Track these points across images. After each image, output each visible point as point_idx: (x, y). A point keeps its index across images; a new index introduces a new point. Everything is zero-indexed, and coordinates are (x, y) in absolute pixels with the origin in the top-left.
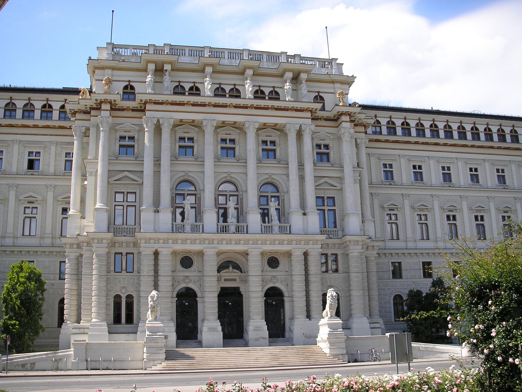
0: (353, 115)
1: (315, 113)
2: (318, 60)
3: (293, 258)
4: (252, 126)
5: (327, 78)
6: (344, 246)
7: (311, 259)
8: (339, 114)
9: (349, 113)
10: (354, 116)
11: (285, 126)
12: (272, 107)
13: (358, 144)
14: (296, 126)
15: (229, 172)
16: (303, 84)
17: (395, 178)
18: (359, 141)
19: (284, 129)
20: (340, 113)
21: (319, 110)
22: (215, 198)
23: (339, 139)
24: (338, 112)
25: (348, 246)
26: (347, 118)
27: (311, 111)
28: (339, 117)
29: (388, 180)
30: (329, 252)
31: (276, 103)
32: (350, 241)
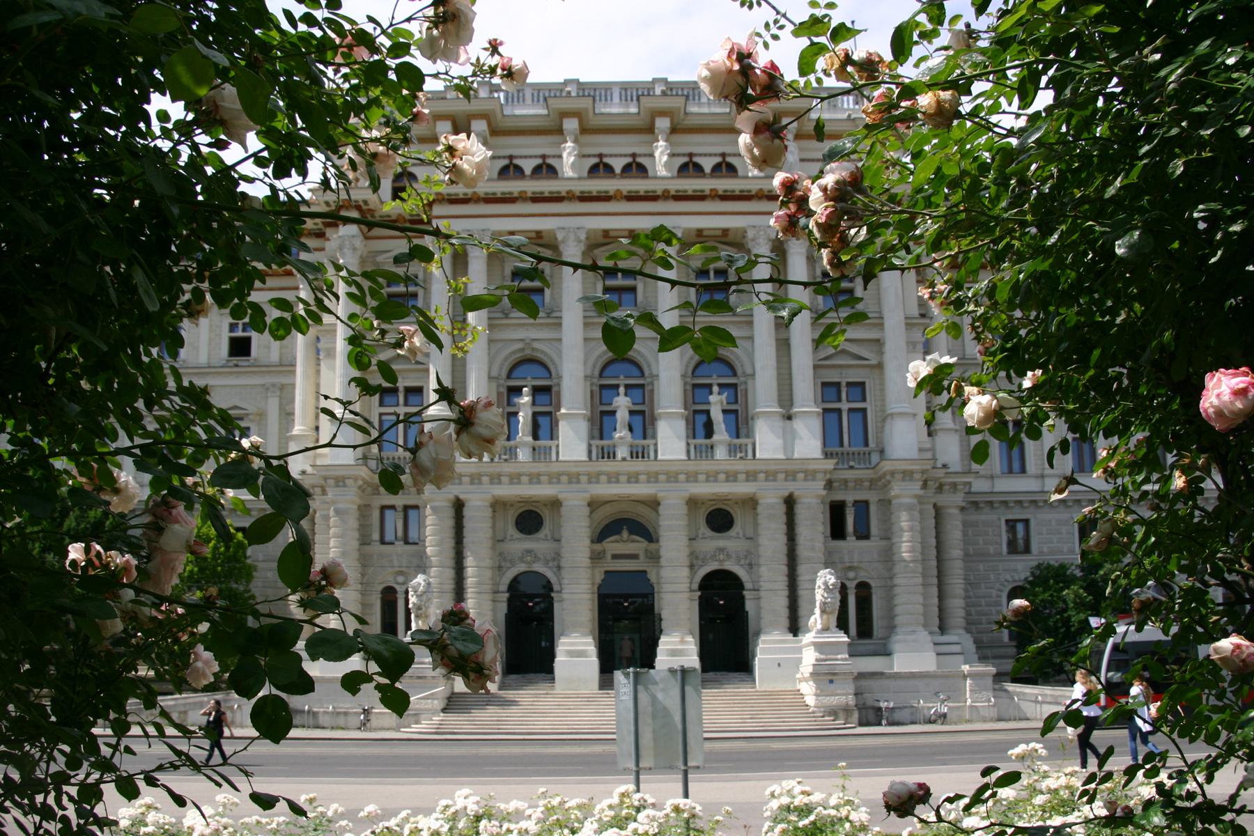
3: (760, 509)
6: (880, 483)
7: (801, 512)
12: (713, 193)
25: (889, 482)
30: (849, 498)
31: (723, 184)
32: (893, 473)
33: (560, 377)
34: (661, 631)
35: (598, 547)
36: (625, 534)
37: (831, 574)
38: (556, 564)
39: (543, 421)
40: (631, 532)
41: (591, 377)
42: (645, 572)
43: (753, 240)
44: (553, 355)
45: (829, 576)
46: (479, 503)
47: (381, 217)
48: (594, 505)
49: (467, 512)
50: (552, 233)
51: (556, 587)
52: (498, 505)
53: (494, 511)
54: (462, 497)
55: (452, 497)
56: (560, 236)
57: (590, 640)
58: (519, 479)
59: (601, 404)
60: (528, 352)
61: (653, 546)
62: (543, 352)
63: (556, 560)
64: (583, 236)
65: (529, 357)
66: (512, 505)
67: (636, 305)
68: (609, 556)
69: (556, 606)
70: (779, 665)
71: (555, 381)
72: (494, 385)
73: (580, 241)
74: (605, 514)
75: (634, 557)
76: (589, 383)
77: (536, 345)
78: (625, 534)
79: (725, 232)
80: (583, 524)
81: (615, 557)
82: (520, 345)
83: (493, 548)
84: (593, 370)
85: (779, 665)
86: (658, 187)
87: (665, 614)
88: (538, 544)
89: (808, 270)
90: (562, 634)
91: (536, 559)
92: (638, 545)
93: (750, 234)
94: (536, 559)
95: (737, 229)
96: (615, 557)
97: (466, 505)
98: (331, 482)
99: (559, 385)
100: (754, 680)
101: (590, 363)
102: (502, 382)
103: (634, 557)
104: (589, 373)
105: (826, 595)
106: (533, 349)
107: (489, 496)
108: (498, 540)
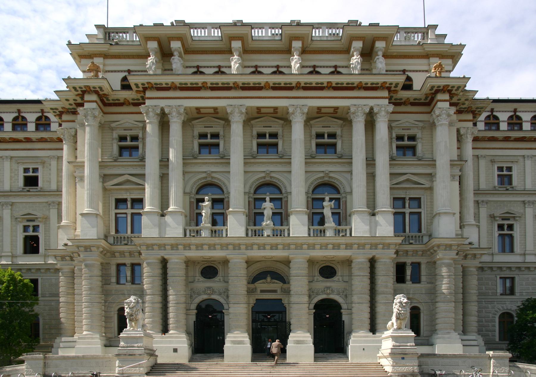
0: (456, 92)
1: (396, 92)
2: (406, 31)
4: (299, 110)
5: (418, 50)
8: (433, 91)
9: (449, 88)
10: (457, 95)
11: (349, 111)
13: (462, 136)
14: (364, 108)
15: (267, 170)
16: (378, 56)
17: (515, 182)
18: (462, 132)
19: (348, 116)
20: (435, 89)
21: (400, 86)
22: (249, 202)
23: (432, 126)
24: (432, 87)
26: (447, 96)
27: (389, 89)
28: (433, 96)
29: (504, 185)
33: (229, 193)
34: (290, 331)
35: (252, 286)
36: (269, 279)
37: (404, 297)
38: (226, 294)
39: (219, 219)
40: (272, 278)
41: (249, 193)
42: (281, 300)
43: (353, 113)
44: (226, 182)
45: (403, 298)
46: (176, 261)
47: (113, 100)
48: (249, 263)
49: (169, 265)
50: (224, 108)
51: (226, 306)
52: (189, 263)
53: (187, 266)
54: (166, 257)
55: (159, 257)
56: (229, 110)
57: (246, 335)
58: (202, 247)
59: (255, 208)
60: (209, 179)
61: (285, 286)
62: (218, 179)
63: (226, 293)
64: (244, 110)
65: (210, 182)
66: (198, 263)
67: (277, 153)
68: (259, 291)
69: (226, 317)
70: (364, 349)
71: (226, 195)
72: (187, 197)
73: (242, 113)
74: (256, 269)
75: (275, 291)
76: (247, 197)
77: (214, 175)
78: (269, 279)
79: (336, 109)
80: (242, 272)
81: (262, 291)
82: (204, 175)
83: (187, 285)
84: (250, 190)
85: (364, 349)
86: (293, 80)
87: (292, 322)
88: (215, 284)
89: (389, 134)
90: (229, 332)
91: (214, 292)
92: (277, 285)
93: (352, 110)
94: (214, 292)
95: (344, 107)
96: (262, 291)
97: (169, 261)
98: (82, 249)
99: (228, 198)
100: (348, 358)
101: (248, 186)
102: (193, 196)
103: (275, 291)
104: (247, 191)
105: (400, 309)
106: (212, 177)
107: (183, 257)
108: (189, 282)
